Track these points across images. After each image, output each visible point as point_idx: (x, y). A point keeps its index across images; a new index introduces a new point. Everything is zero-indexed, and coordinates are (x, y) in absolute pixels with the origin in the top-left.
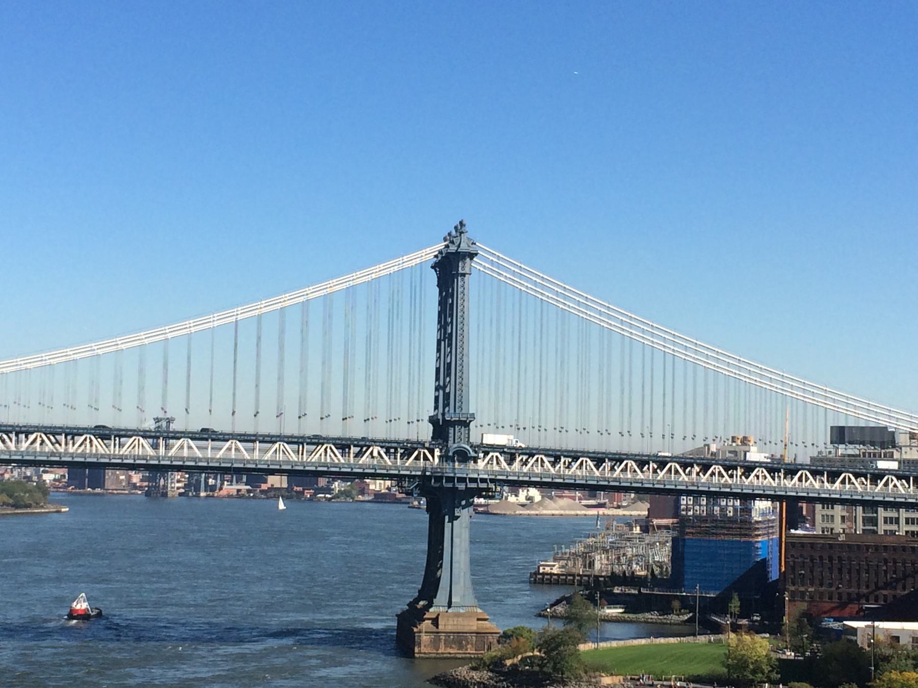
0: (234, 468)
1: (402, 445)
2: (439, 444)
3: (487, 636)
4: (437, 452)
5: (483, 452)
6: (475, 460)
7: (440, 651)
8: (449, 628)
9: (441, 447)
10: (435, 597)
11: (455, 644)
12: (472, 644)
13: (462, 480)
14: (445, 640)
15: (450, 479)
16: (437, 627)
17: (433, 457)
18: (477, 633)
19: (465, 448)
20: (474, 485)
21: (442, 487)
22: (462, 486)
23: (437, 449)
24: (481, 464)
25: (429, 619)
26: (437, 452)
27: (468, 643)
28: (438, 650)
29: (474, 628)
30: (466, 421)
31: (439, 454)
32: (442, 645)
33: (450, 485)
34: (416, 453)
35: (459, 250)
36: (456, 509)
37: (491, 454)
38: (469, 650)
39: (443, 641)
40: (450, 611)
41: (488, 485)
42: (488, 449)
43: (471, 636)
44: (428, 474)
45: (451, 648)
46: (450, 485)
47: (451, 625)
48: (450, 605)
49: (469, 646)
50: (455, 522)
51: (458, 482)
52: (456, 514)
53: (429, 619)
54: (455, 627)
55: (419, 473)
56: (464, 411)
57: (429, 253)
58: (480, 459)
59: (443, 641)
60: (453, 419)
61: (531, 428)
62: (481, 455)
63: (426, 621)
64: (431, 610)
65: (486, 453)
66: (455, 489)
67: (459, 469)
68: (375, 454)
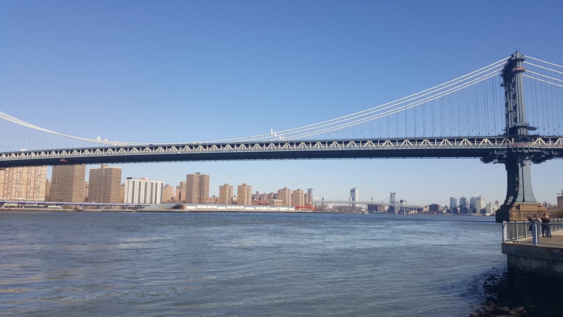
1: (497, 137)
4: (513, 140)
5: (534, 139)
8: (525, 210)
10: (517, 198)
13: (526, 149)
14: (523, 215)
15: (520, 149)
16: (519, 210)
17: (511, 142)
18: (538, 212)
20: (532, 151)
21: (518, 152)
22: (526, 151)
23: (513, 138)
25: (515, 206)
26: (513, 140)
29: (537, 210)
30: (525, 126)
31: (514, 140)
33: (521, 151)
34: (504, 140)
35: (517, 58)
36: (524, 161)
40: (524, 203)
41: (538, 151)
44: (510, 147)
46: (521, 151)
48: (524, 201)
50: (523, 167)
51: (524, 150)
52: (524, 164)
53: (515, 206)
54: (528, 209)
55: (507, 148)
56: (524, 122)
57: (503, 62)
60: (520, 125)
63: (514, 207)
64: (515, 203)
65: (535, 140)
66: (523, 153)
68: (486, 142)
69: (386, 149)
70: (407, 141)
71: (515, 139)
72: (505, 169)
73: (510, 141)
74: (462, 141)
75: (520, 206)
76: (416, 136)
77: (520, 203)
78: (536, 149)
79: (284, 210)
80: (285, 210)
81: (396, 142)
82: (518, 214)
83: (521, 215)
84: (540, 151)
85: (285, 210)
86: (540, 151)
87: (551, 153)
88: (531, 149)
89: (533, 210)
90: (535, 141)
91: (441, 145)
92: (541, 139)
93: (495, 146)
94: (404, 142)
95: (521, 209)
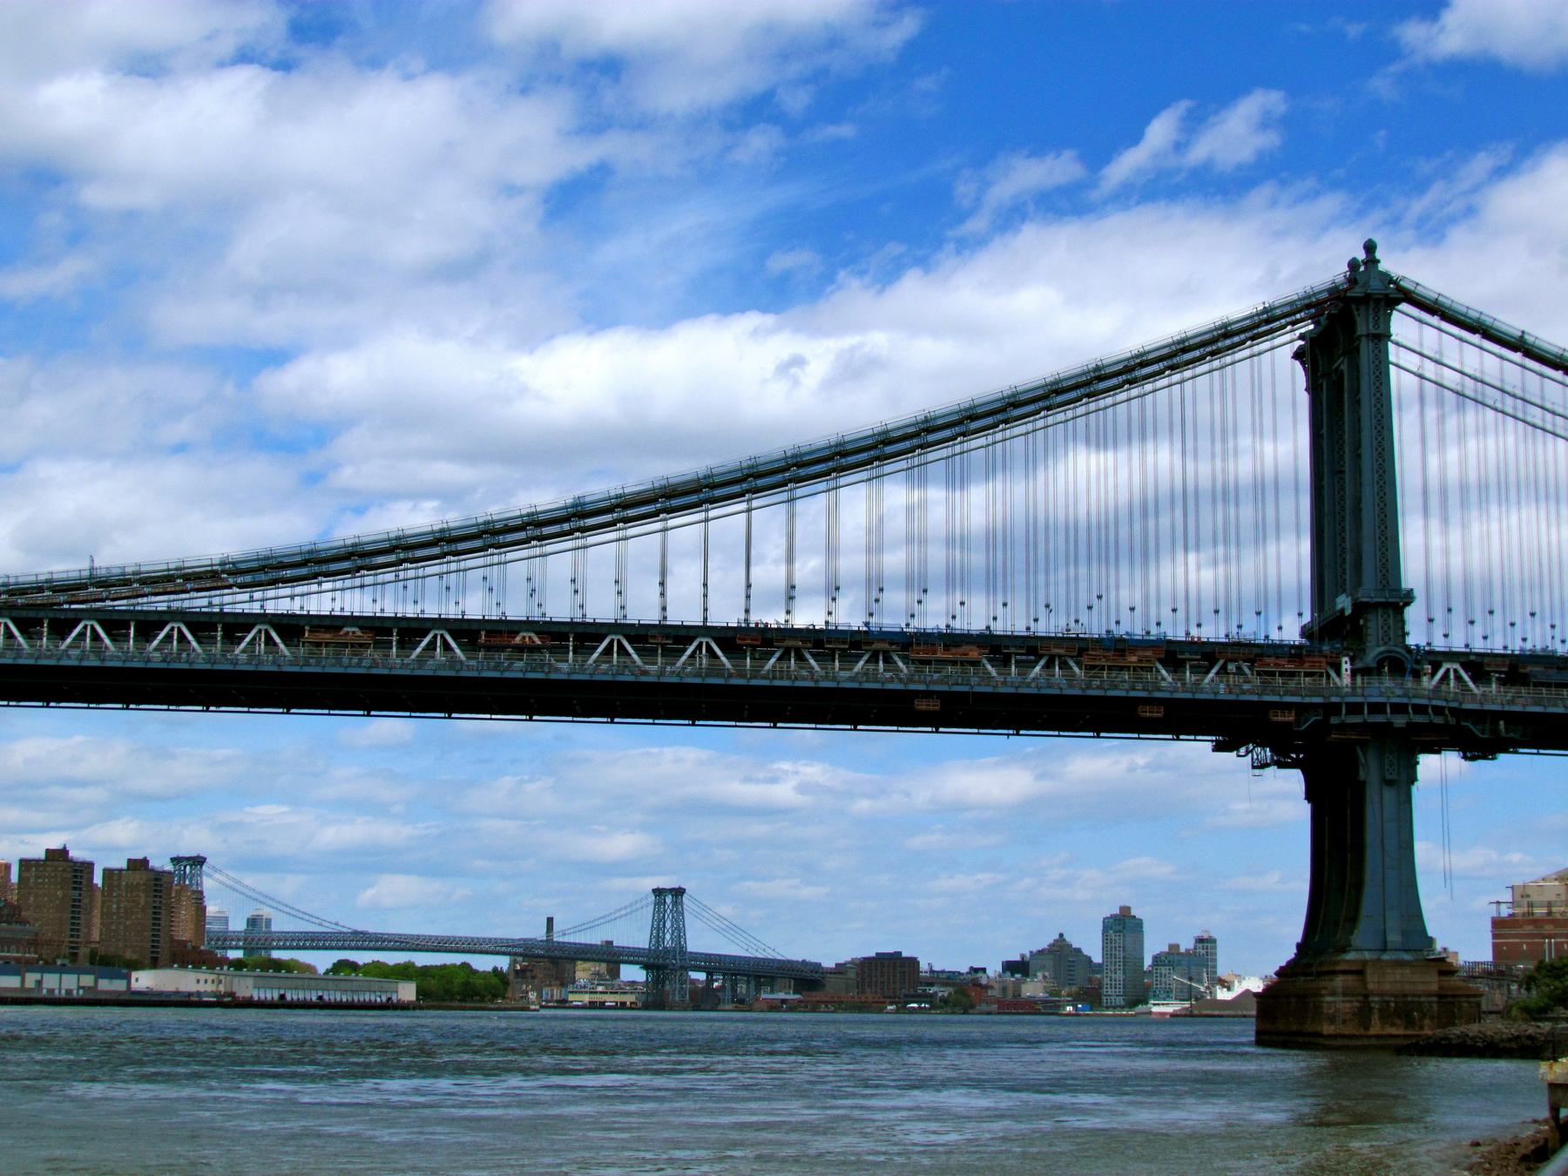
0: (974, 693)
2: (1347, 649)
3: (1459, 1002)
4: (1346, 666)
6: (1417, 675)
7: (1372, 1031)
9: (1351, 654)
11: (1400, 1017)
12: (1432, 1018)
13: (1399, 709)
14: (1381, 1010)
17: (1339, 674)
19: (1398, 653)
23: (1346, 659)
24: (1428, 683)
26: (1346, 666)
27: (1423, 1016)
28: (1367, 1028)
31: (1348, 666)
32: (1375, 1019)
37: (1446, 666)
38: (1426, 1028)
39: (1376, 1011)
42: (1435, 659)
43: (1430, 1002)
44: (1334, 699)
45: (1393, 1025)
47: (1391, 983)
49: (1427, 1022)
52: (1388, 777)
54: (1399, 985)
58: (1425, 674)
59: (1376, 1011)
61: (1509, 627)
62: (1428, 668)
65: (1436, 666)
67: (1386, 689)
69: (427, 671)
70: (707, 643)
71: (1352, 660)
72: (1304, 796)
73: (1333, 674)
74: (249, 632)
75: (1369, 972)
76: (831, 619)
77: (1367, 956)
78: (1438, 710)
79: (64, 986)
80: (73, 986)
81: (392, 636)
82: (1360, 1009)
83: (1371, 1009)
84: (1452, 721)
85: (73, 986)
86: (1452, 721)
87: (1495, 731)
88: (1420, 709)
89: (1421, 988)
90: (1433, 674)
91: (154, 652)
92: (1457, 666)
93: (741, 674)
94: (695, 644)
95: (1371, 986)
